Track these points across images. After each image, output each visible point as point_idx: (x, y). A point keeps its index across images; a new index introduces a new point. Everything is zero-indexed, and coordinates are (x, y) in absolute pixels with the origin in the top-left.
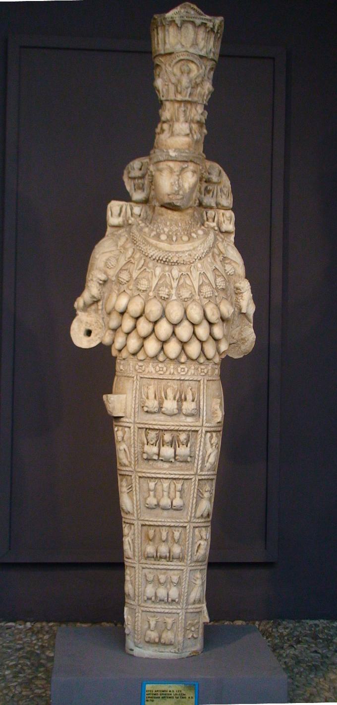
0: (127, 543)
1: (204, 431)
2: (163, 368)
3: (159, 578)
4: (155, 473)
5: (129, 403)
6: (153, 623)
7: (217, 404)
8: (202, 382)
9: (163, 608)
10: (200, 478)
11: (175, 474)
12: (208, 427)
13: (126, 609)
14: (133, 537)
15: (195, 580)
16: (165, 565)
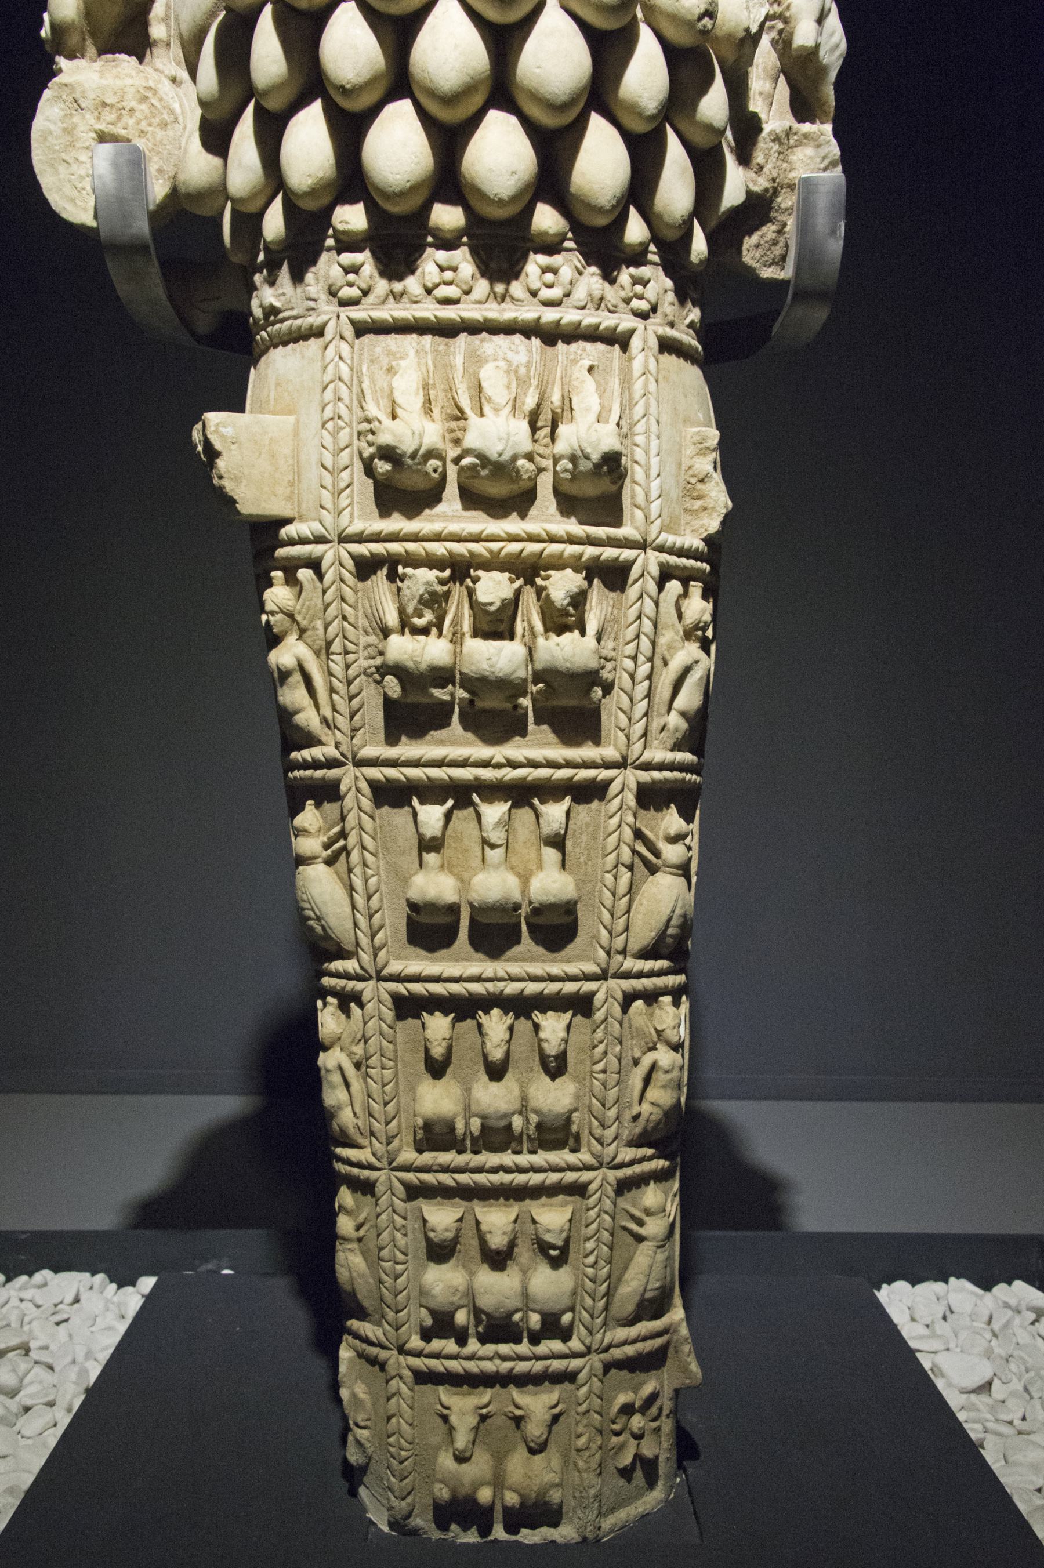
0: (336, 1078)
1: (655, 571)
2: (455, 269)
3: (484, 1227)
4: (439, 764)
5: (311, 454)
6: (463, 1423)
7: (703, 452)
8: (636, 343)
9: (504, 1358)
10: (645, 776)
11: (534, 764)
12: (671, 551)
13: (345, 1353)
14: (359, 1050)
15: (641, 1223)
16: (507, 1170)
